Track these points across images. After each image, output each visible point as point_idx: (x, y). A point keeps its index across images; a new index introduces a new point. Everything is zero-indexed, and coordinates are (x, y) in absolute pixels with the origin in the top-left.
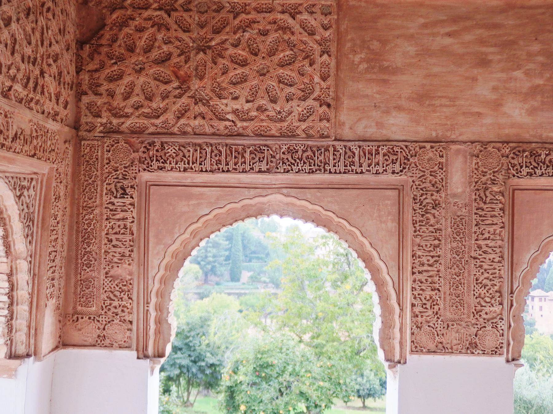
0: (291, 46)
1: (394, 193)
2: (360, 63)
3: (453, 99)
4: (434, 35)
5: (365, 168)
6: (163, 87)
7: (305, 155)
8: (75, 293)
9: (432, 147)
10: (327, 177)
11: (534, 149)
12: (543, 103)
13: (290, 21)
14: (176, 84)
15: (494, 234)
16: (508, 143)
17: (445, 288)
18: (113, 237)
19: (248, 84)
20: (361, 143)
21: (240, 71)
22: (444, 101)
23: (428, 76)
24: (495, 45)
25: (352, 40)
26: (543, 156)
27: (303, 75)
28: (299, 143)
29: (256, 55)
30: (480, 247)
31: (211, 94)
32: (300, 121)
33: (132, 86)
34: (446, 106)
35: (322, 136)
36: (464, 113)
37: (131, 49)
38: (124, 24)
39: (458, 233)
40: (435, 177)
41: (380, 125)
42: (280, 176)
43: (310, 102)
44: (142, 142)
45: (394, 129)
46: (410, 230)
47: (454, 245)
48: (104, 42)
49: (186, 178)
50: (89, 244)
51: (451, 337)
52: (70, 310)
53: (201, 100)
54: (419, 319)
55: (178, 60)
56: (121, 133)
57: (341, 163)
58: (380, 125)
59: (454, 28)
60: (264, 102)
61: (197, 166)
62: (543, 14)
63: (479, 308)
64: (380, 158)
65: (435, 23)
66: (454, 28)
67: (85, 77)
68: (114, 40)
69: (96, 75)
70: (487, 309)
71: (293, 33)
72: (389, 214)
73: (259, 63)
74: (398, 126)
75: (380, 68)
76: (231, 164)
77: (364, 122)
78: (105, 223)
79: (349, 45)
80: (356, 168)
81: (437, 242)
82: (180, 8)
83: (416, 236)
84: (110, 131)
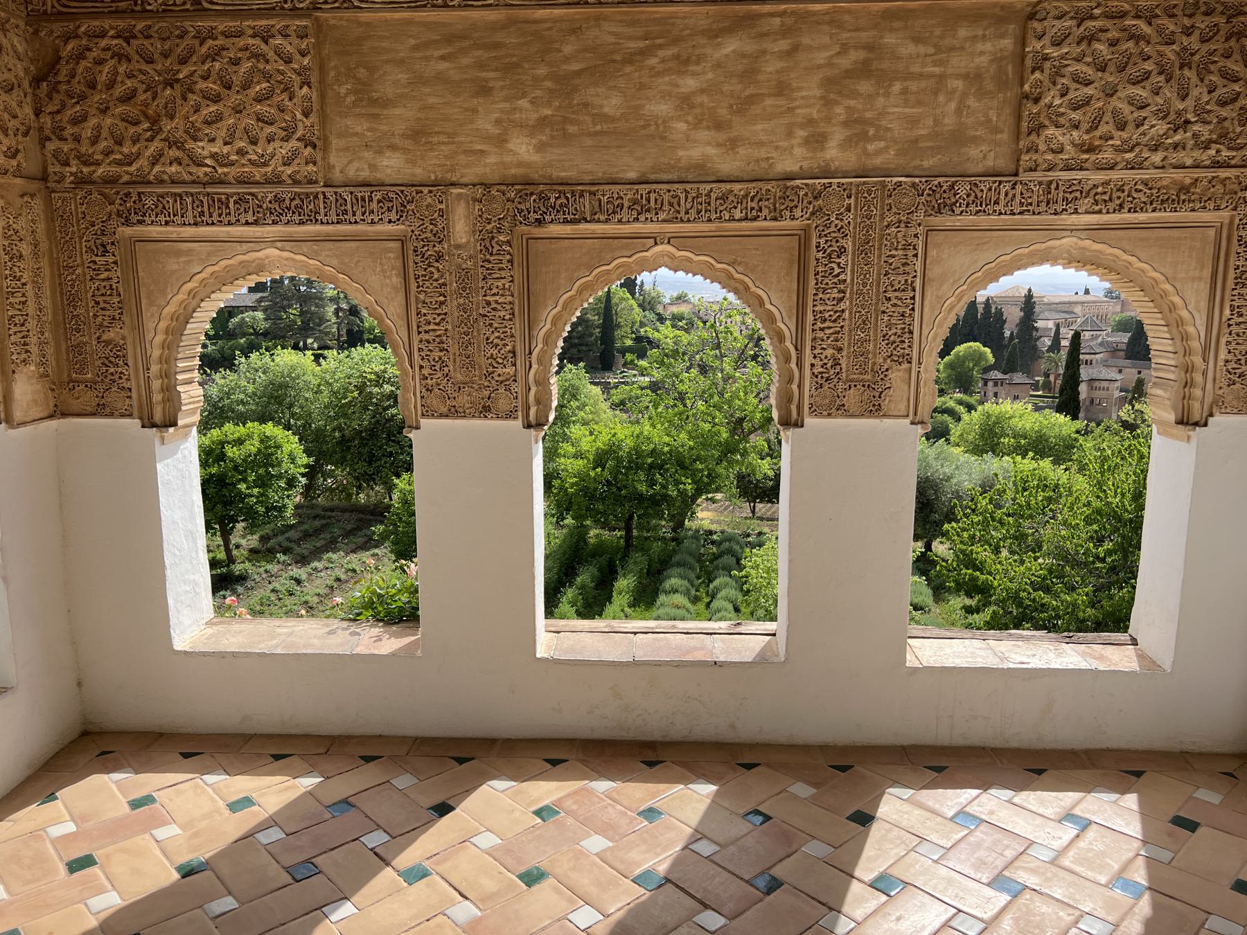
0: (267, 77)
1: (396, 245)
2: (347, 95)
3: (449, 135)
4: (427, 59)
5: (358, 217)
6: (132, 130)
7: (294, 203)
8: (68, 360)
9: (430, 192)
10: (318, 227)
11: (542, 192)
12: (552, 137)
13: (263, 46)
14: (146, 125)
15: (504, 289)
16: (513, 185)
17: (454, 348)
18: (100, 299)
19: (224, 123)
20: (352, 189)
21: (213, 108)
22: (443, 138)
23: (421, 109)
24: (496, 70)
25: (336, 67)
26: (552, 200)
27: (283, 111)
28: (286, 191)
29: (229, 88)
30: (489, 303)
31: (184, 135)
32: (284, 164)
33: (98, 128)
34: (444, 143)
35: (310, 182)
36: (465, 152)
37: (92, 86)
38: (80, 56)
39: (464, 289)
40: (435, 225)
41: (373, 167)
42: (268, 228)
43: (294, 143)
44: (118, 193)
45: (389, 171)
46: (413, 286)
47: (461, 301)
48: (61, 78)
49: (172, 233)
50: (75, 307)
51: (463, 400)
52: (65, 378)
53: (175, 143)
54: (429, 381)
55: (144, 97)
56: (93, 182)
57: (333, 212)
58: (373, 167)
59: (450, 49)
60: (243, 144)
61: (178, 219)
62: (550, 29)
63: (491, 369)
64: (374, 205)
65: (426, 45)
66: (450, 49)
67: (46, 120)
68: (72, 75)
69: (58, 117)
70: (500, 371)
71: (267, 61)
72: (393, 268)
73: (234, 98)
74: (392, 166)
75: (371, 103)
76: (215, 214)
77: (356, 165)
78: (89, 284)
79: (332, 74)
80: (349, 217)
81: (442, 298)
82: (139, 35)
83: (419, 293)
84: (81, 182)
